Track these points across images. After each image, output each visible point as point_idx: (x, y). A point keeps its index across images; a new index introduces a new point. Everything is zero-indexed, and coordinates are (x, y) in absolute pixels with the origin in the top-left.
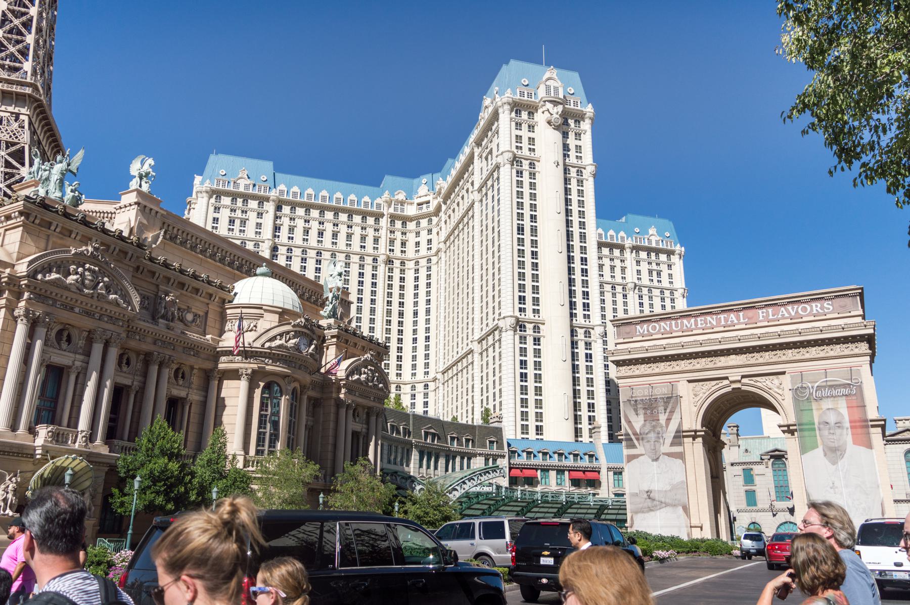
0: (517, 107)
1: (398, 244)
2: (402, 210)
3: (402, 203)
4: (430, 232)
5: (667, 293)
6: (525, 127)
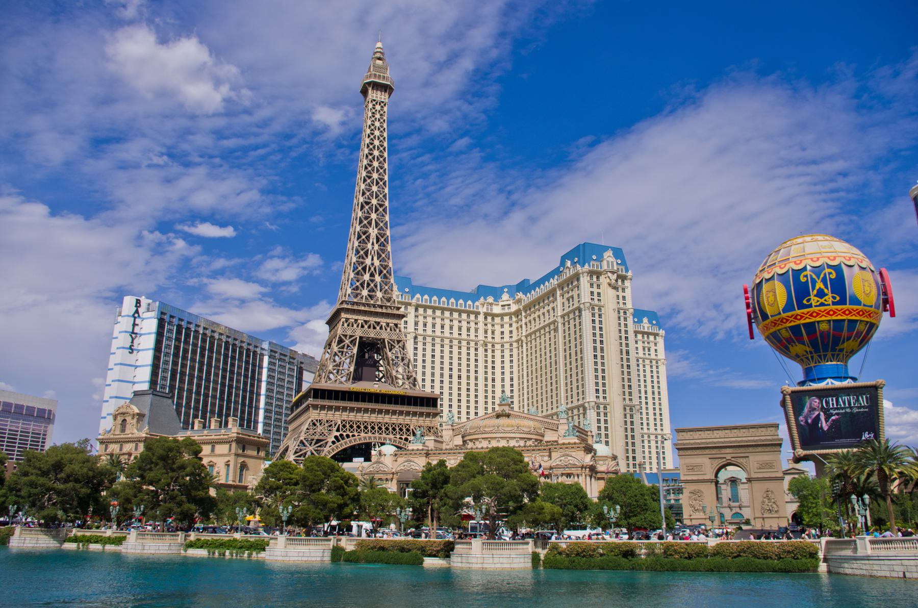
0: (591, 273)
1: (489, 332)
2: (492, 309)
3: (491, 304)
4: (511, 325)
5: (654, 362)
6: (595, 286)
